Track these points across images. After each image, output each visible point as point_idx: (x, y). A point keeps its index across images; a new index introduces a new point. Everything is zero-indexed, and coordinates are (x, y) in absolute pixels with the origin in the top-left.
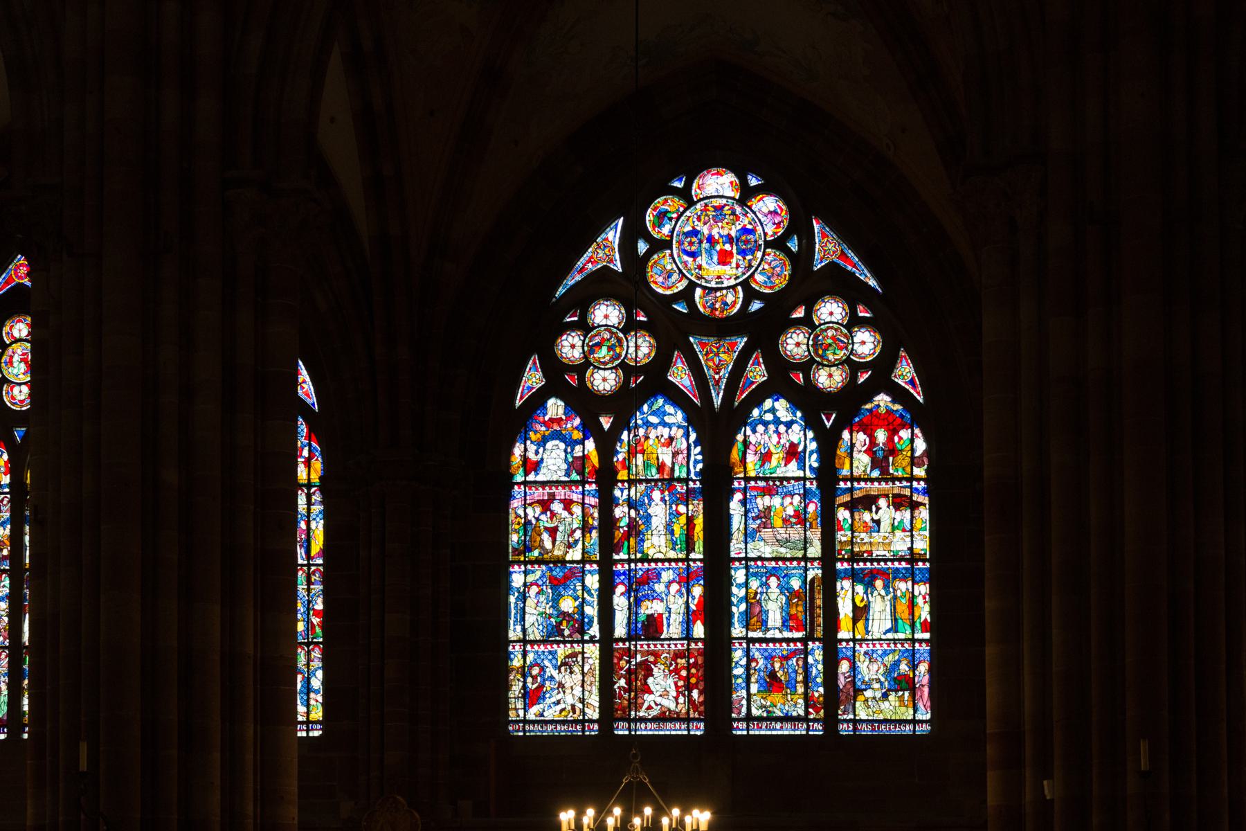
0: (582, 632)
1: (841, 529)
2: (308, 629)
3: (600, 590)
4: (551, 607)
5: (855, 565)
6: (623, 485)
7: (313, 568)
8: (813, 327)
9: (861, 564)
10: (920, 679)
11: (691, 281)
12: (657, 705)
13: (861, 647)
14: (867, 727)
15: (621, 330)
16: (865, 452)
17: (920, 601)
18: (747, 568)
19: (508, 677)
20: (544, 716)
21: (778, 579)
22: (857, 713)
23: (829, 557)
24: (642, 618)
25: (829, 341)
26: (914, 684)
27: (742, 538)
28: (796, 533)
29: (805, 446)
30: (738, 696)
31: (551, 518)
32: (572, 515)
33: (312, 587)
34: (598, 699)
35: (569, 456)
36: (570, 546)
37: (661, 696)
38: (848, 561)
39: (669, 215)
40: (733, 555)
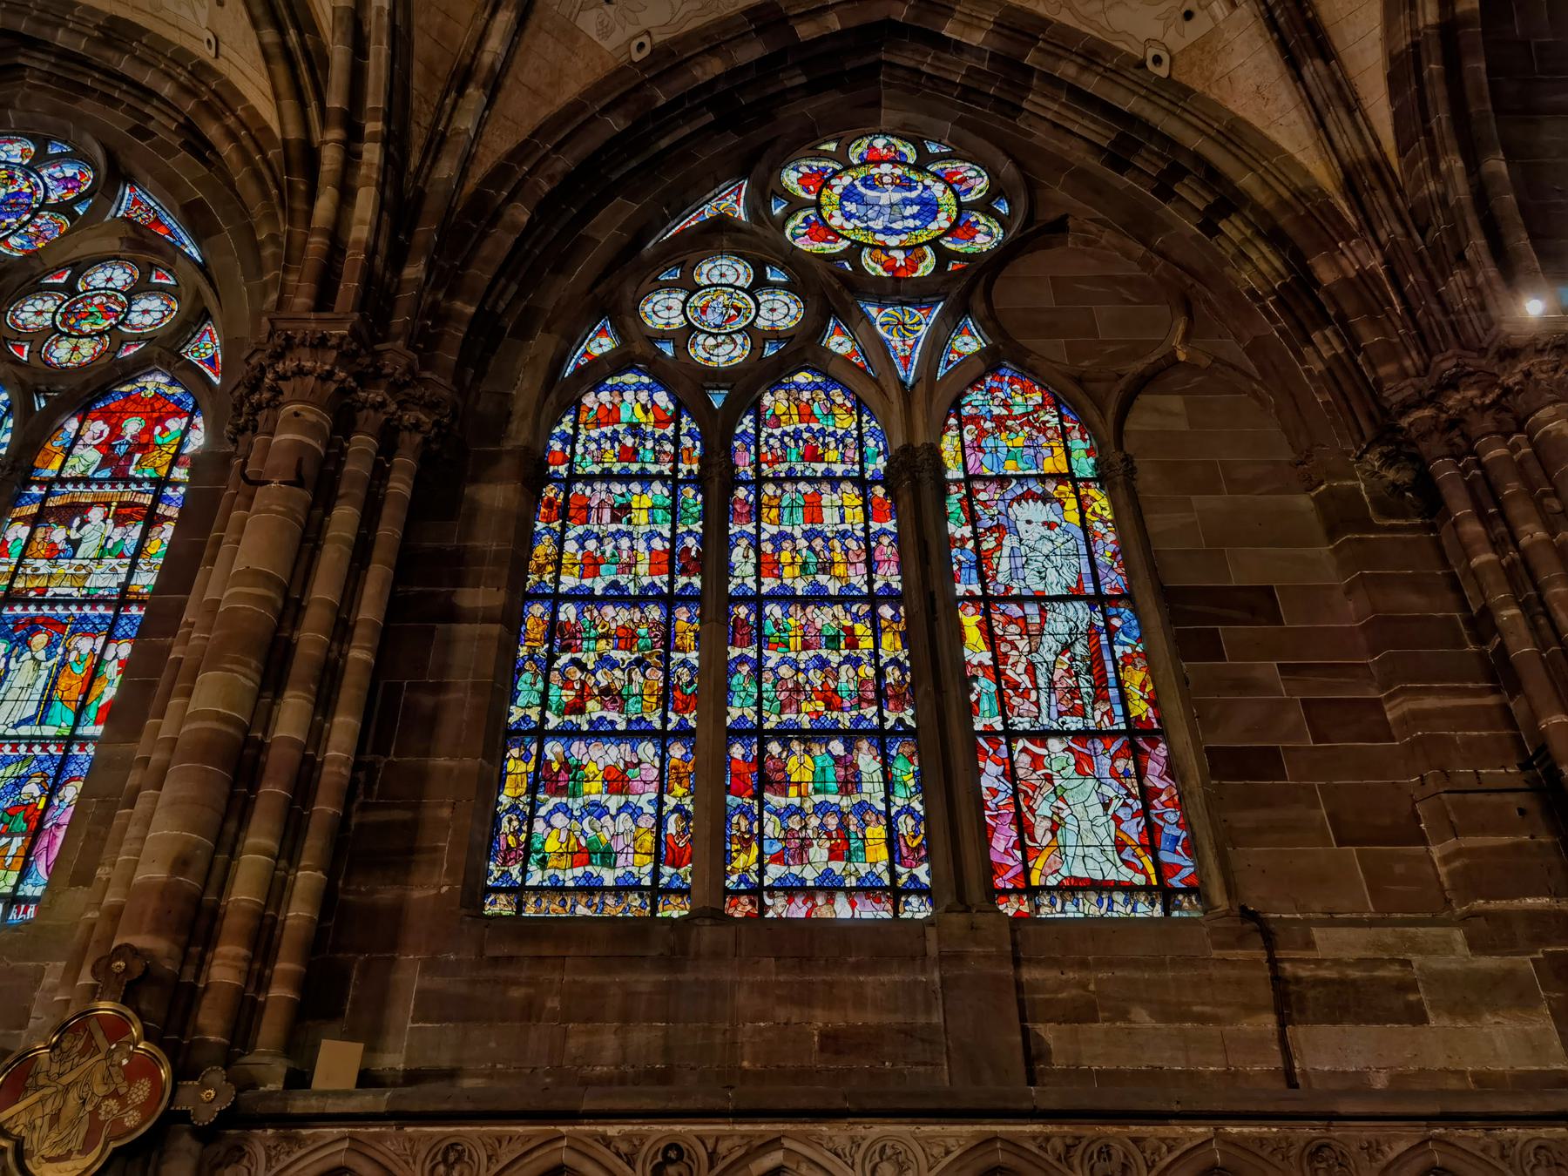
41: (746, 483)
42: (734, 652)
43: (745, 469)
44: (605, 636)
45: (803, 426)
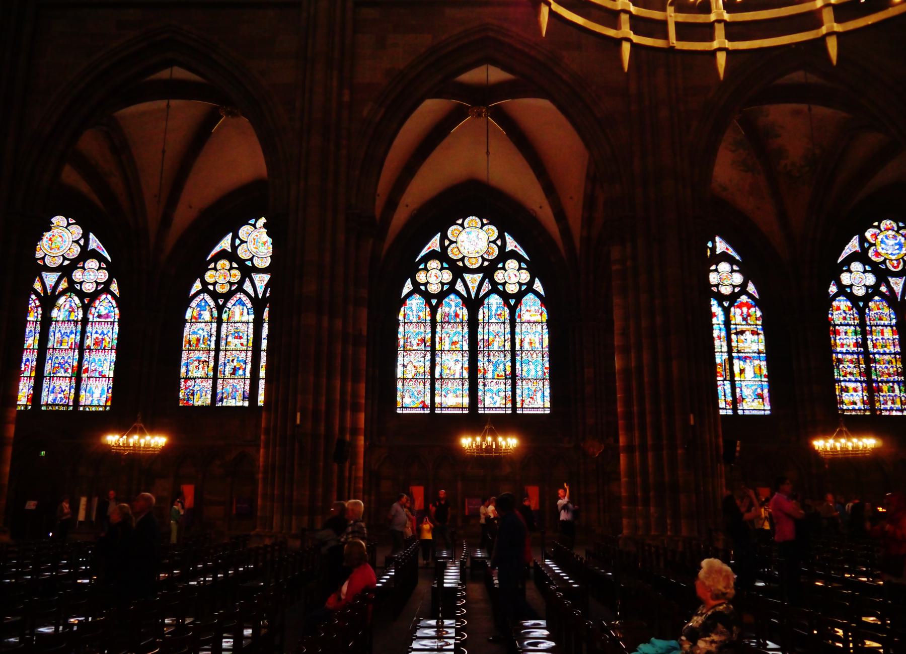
7: (544, 352)
17: (763, 367)
25: (725, 277)
41: (868, 326)
42: (872, 365)
43: (868, 323)
44: (847, 361)
45: (878, 311)
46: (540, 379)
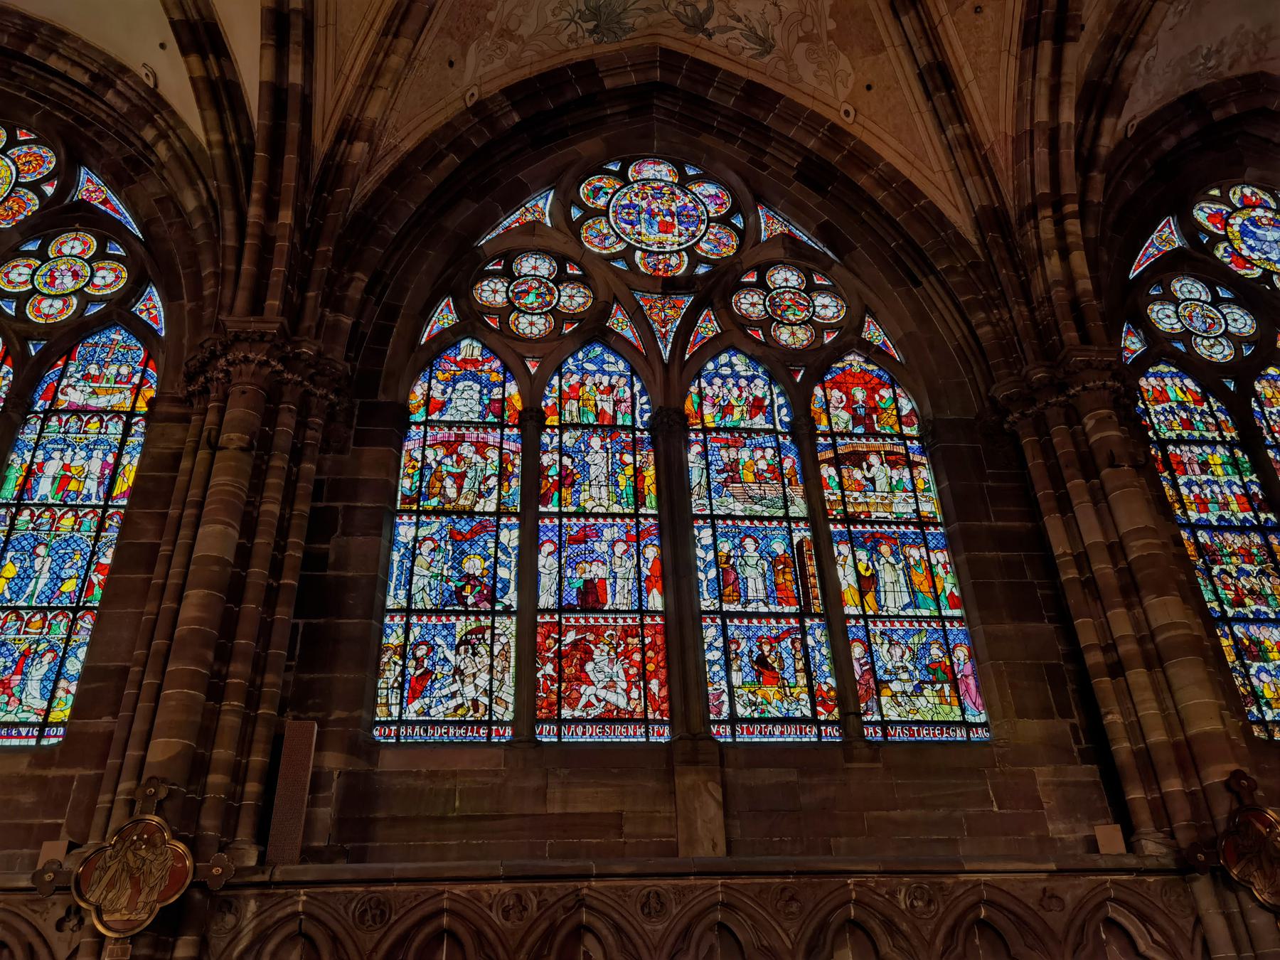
0: (493, 600)
1: (828, 487)
2: (81, 590)
3: (520, 547)
4: (452, 567)
5: (852, 527)
6: (553, 431)
7: (111, 511)
8: (769, 291)
9: (860, 527)
10: (961, 667)
11: (629, 244)
12: (599, 700)
13: (875, 625)
14: (903, 733)
15: (551, 281)
16: (843, 408)
17: (940, 570)
18: (714, 527)
19: (379, 659)
20: (429, 715)
21: (756, 541)
22: (884, 713)
23: (817, 517)
24: (580, 584)
25: (788, 303)
26: (955, 675)
27: (704, 492)
28: (772, 491)
29: (772, 401)
30: (716, 689)
31: (458, 462)
32: (486, 459)
33: (103, 534)
34: (512, 692)
35: (485, 397)
36: (480, 495)
37: (605, 687)
38: (841, 522)
39: (604, 190)
40: (695, 511)
46: (63, 609)
